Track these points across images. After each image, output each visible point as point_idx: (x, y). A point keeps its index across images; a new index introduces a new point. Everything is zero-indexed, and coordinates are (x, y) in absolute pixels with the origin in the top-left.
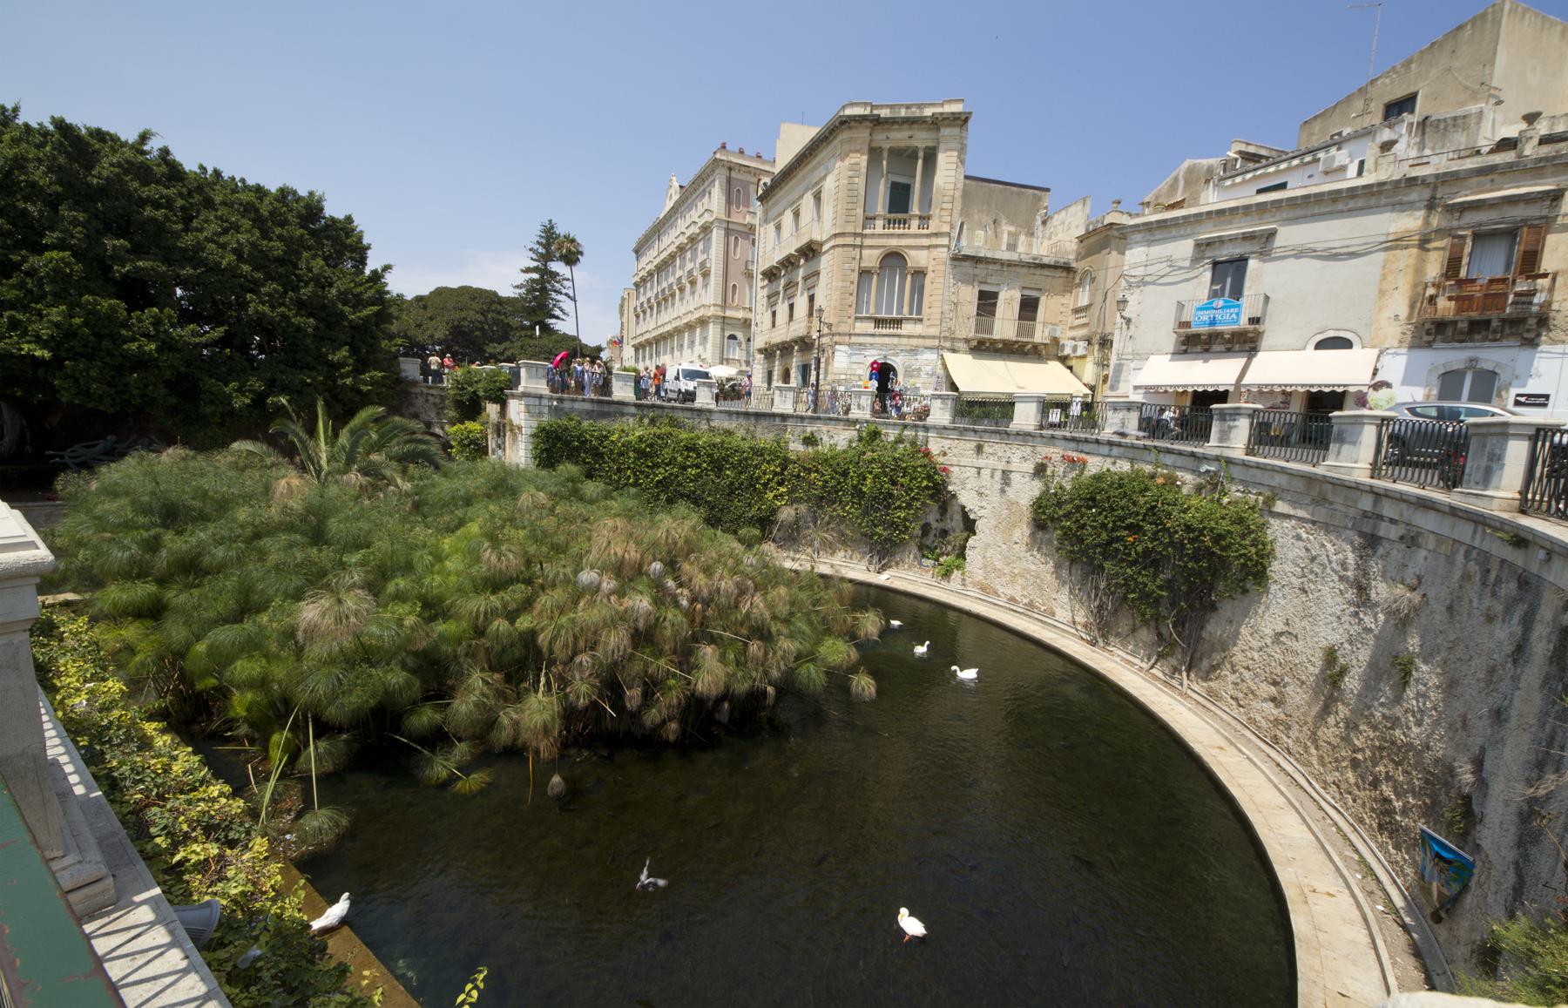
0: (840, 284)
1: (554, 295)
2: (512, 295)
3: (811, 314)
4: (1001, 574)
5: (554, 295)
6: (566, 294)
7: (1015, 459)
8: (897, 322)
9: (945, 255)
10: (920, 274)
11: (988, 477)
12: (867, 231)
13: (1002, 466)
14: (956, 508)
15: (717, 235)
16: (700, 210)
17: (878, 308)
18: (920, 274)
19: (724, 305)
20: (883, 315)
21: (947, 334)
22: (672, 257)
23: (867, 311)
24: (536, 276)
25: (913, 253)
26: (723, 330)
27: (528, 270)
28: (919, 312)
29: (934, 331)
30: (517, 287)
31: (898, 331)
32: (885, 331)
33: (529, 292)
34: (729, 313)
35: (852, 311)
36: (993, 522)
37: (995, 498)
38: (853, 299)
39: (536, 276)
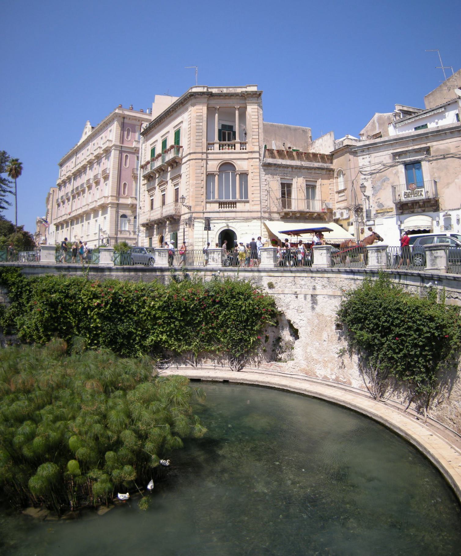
0: (195, 182)
3: (177, 200)
7: (318, 287)
8: (234, 203)
9: (258, 164)
10: (244, 175)
11: (303, 299)
12: (210, 151)
13: (311, 292)
15: (114, 154)
16: (104, 140)
17: (220, 196)
18: (244, 175)
19: (118, 195)
20: (224, 200)
21: (266, 210)
22: (84, 168)
23: (214, 198)
26: (117, 212)
28: (246, 197)
29: (257, 208)
31: (234, 209)
32: (225, 209)
34: (122, 201)
35: (204, 197)
36: (309, 329)
37: (309, 313)
38: (204, 190)
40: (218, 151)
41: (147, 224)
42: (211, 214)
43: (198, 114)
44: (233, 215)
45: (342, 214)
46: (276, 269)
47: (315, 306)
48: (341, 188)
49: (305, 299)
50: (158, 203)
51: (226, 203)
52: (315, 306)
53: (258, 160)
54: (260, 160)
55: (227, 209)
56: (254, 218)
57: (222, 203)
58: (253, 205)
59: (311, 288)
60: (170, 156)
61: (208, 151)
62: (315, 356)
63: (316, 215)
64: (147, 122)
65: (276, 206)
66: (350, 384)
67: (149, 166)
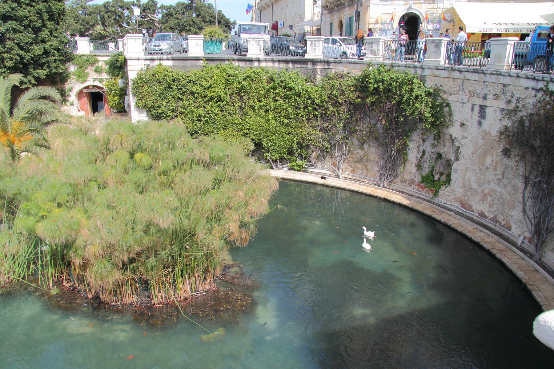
4: (475, 192)
11: (470, 109)
13: (478, 102)
14: (448, 137)
47: (483, 121)
49: (472, 110)
52: (483, 121)
59: (481, 96)
62: (474, 186)
66: (509, 228)
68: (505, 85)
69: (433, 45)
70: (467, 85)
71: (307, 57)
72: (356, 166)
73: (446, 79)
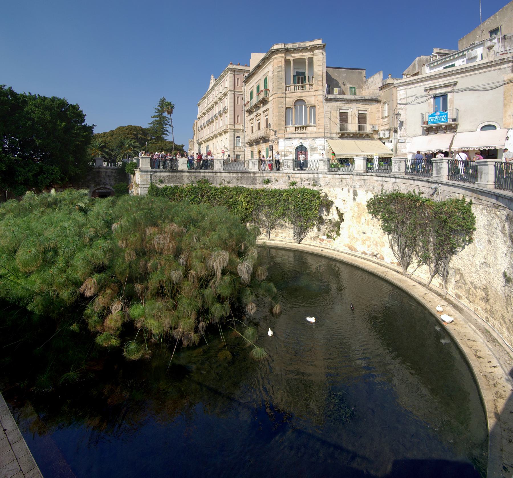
0: (278, 114)
1: (164, 126)
2: (148, 127)
3: (267, 127)
5: (164, 126)
6: (170, 125)
8: (305, 127)
10: (313, 107)
17: (296, 122)
24: (157, 119)
25: (308, 98)
27: (153, 117)
28: (315, 123)
29: (321, 130)
30: (150, 124)
32: (300, 132)
33: (154, 125)
35: (284, 124)
38: (284, 119)
39: (157, 119)
40: (293, 91)
41: (249, 143)
42: (290, 135)
43: (279, 65)
44: (305, 136)
45: (384, 134)
46: (329, 173)
48: (386, 114)
50: (255, 128)
51: (300, 127)
53: (322, 96)
54: (323, 96)
55: (301, 132)
56: (319, 138)
57: (297, 127)
58: (319, 129)
59: (353, 187)
60: (262, 96)
61: (286, 92)
63: (364, 135)
64: (247, 72)
65: (336, 129)
67: (249, 104)
68: (364, 180)
69: (322, 162)
70: (344, 181)
71: (250, 170)
72: (278, 232)
73: (331, 179)
